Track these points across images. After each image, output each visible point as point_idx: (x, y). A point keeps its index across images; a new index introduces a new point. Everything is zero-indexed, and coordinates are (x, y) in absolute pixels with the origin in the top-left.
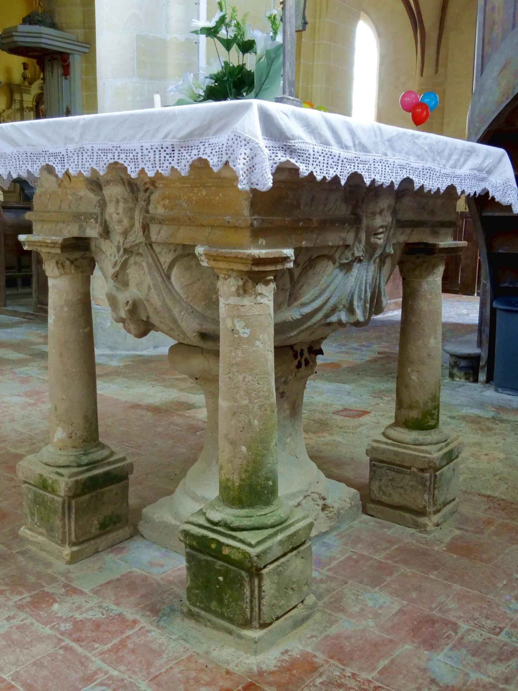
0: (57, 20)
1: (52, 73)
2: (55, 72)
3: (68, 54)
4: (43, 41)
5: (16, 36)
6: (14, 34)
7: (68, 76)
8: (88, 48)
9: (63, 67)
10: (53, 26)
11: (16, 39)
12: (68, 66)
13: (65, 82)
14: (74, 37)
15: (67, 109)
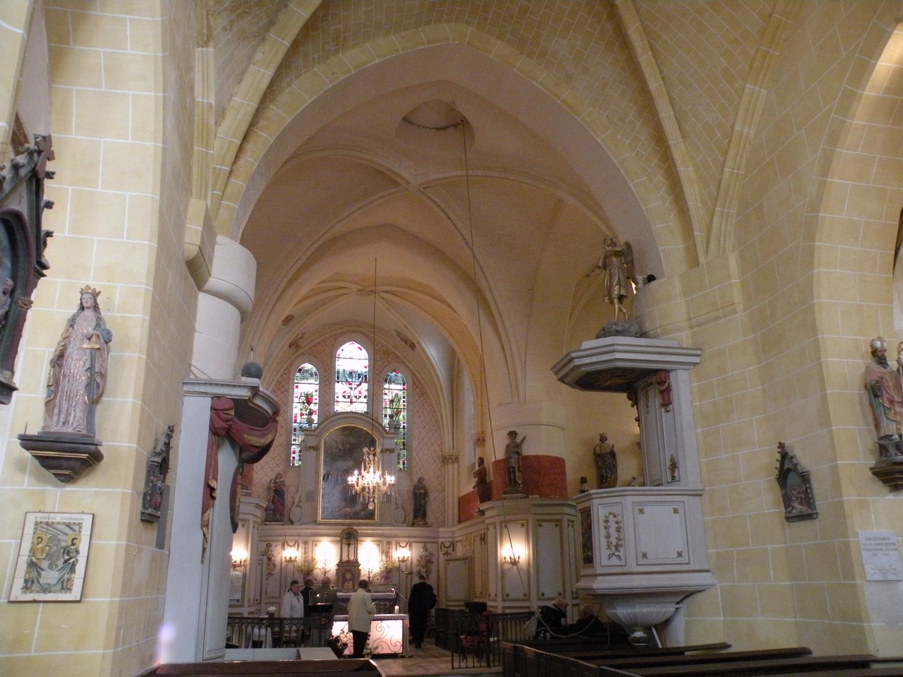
0: (648, 326)
1: (647, 407)
2: (651, 404)
3: (668, 371)
4: (618, 356)
5: (578, 358)
6: (573, 355)
7: (670, 406)
8: (699, 355)
9: (662, 392)
10: (643, 334)
11: (577, 362)
12: (668, 390)
13: (666, 417)
14: (675, 344)
15: (672, 459)
